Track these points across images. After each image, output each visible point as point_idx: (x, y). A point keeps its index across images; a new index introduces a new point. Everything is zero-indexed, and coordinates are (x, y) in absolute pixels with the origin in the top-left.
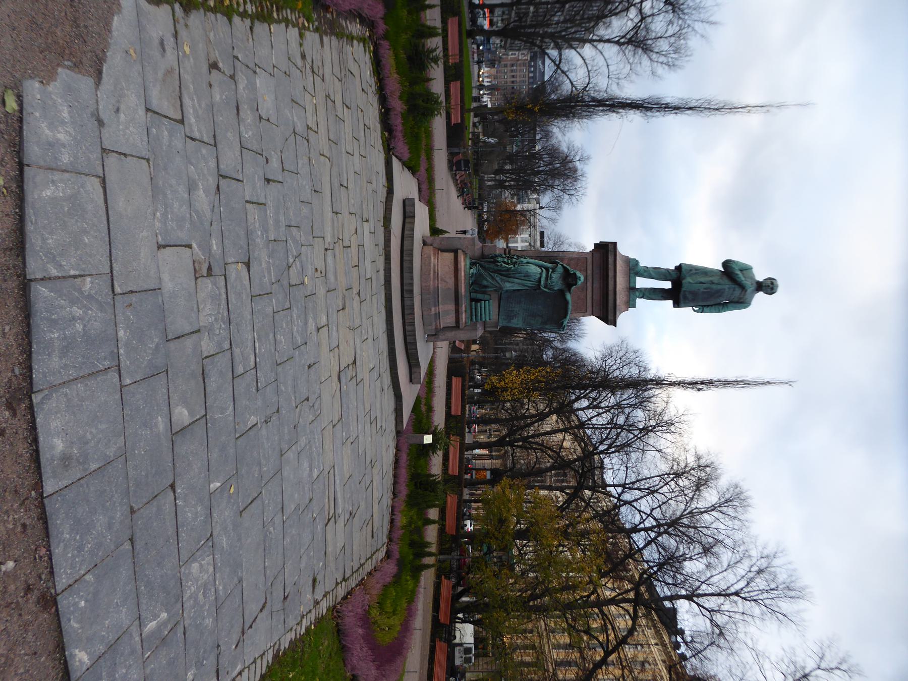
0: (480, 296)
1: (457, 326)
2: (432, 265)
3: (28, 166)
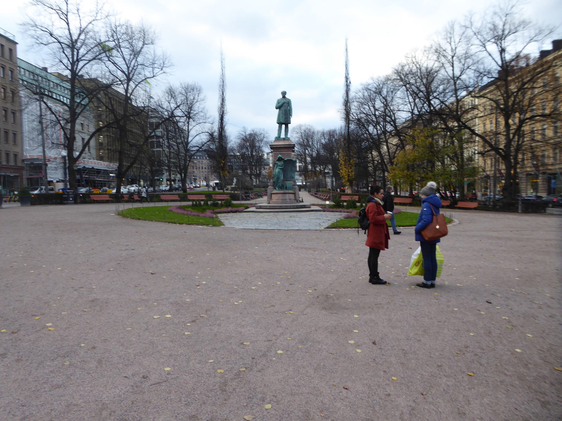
1: (294, 194)
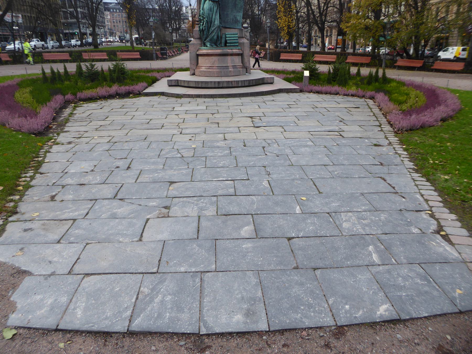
0: (223, 41)
1: (241, 55)
2: (205, 70)
3: (58, 326)
